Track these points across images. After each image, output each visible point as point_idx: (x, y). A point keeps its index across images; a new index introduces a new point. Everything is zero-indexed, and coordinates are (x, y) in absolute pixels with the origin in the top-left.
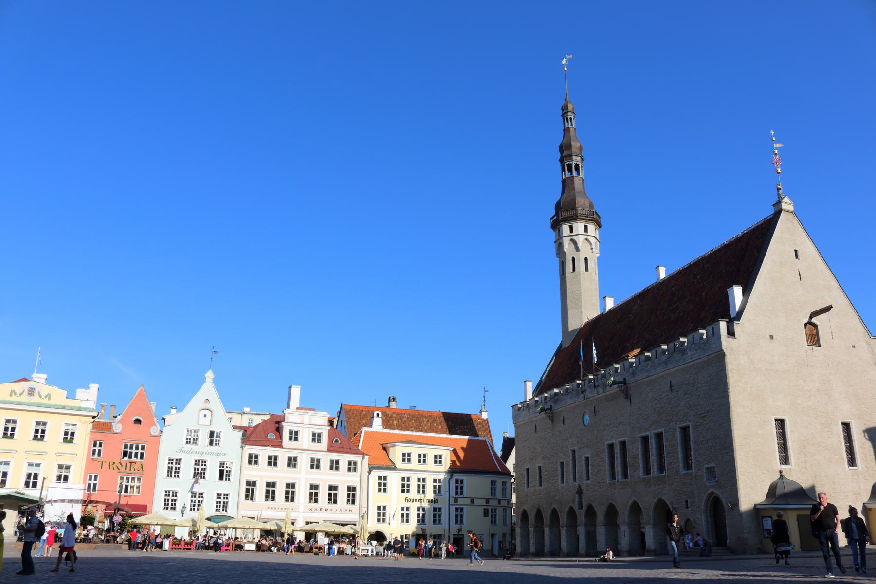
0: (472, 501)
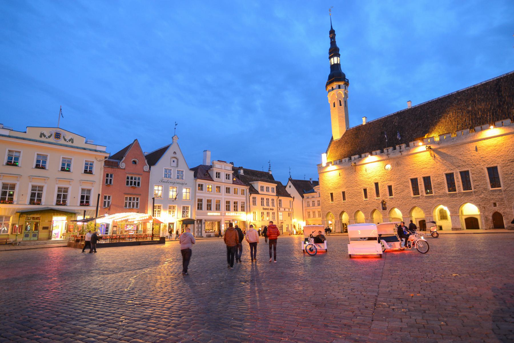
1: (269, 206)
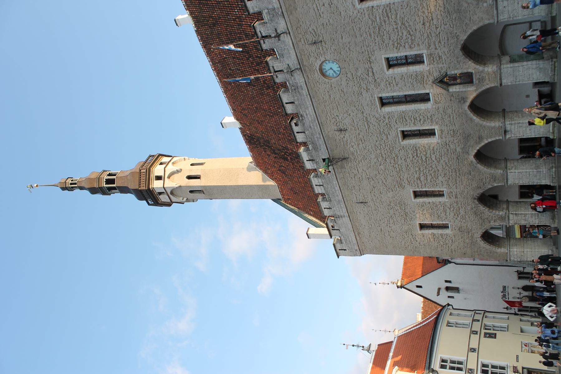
0: (473, 350)
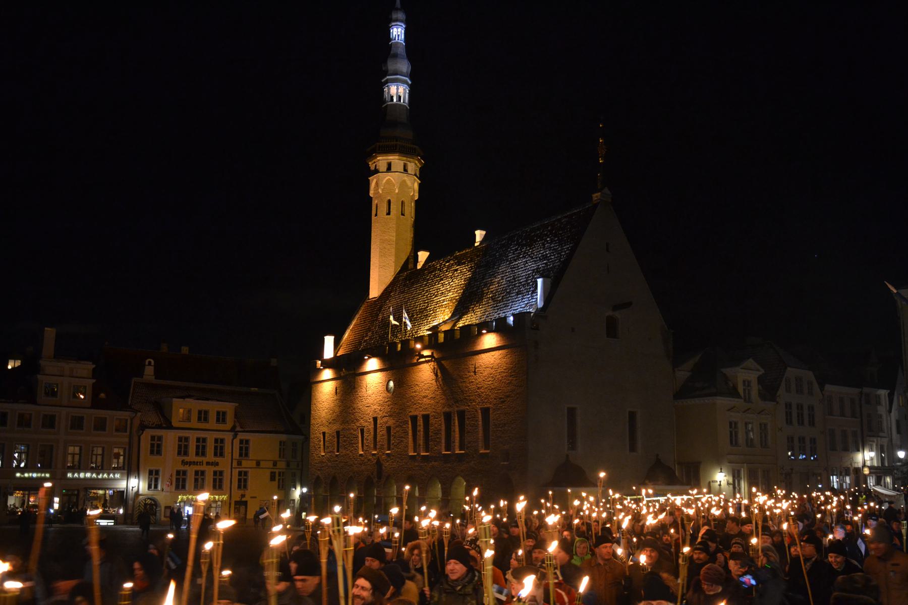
0: (258, 463)
1: (204, 454)
